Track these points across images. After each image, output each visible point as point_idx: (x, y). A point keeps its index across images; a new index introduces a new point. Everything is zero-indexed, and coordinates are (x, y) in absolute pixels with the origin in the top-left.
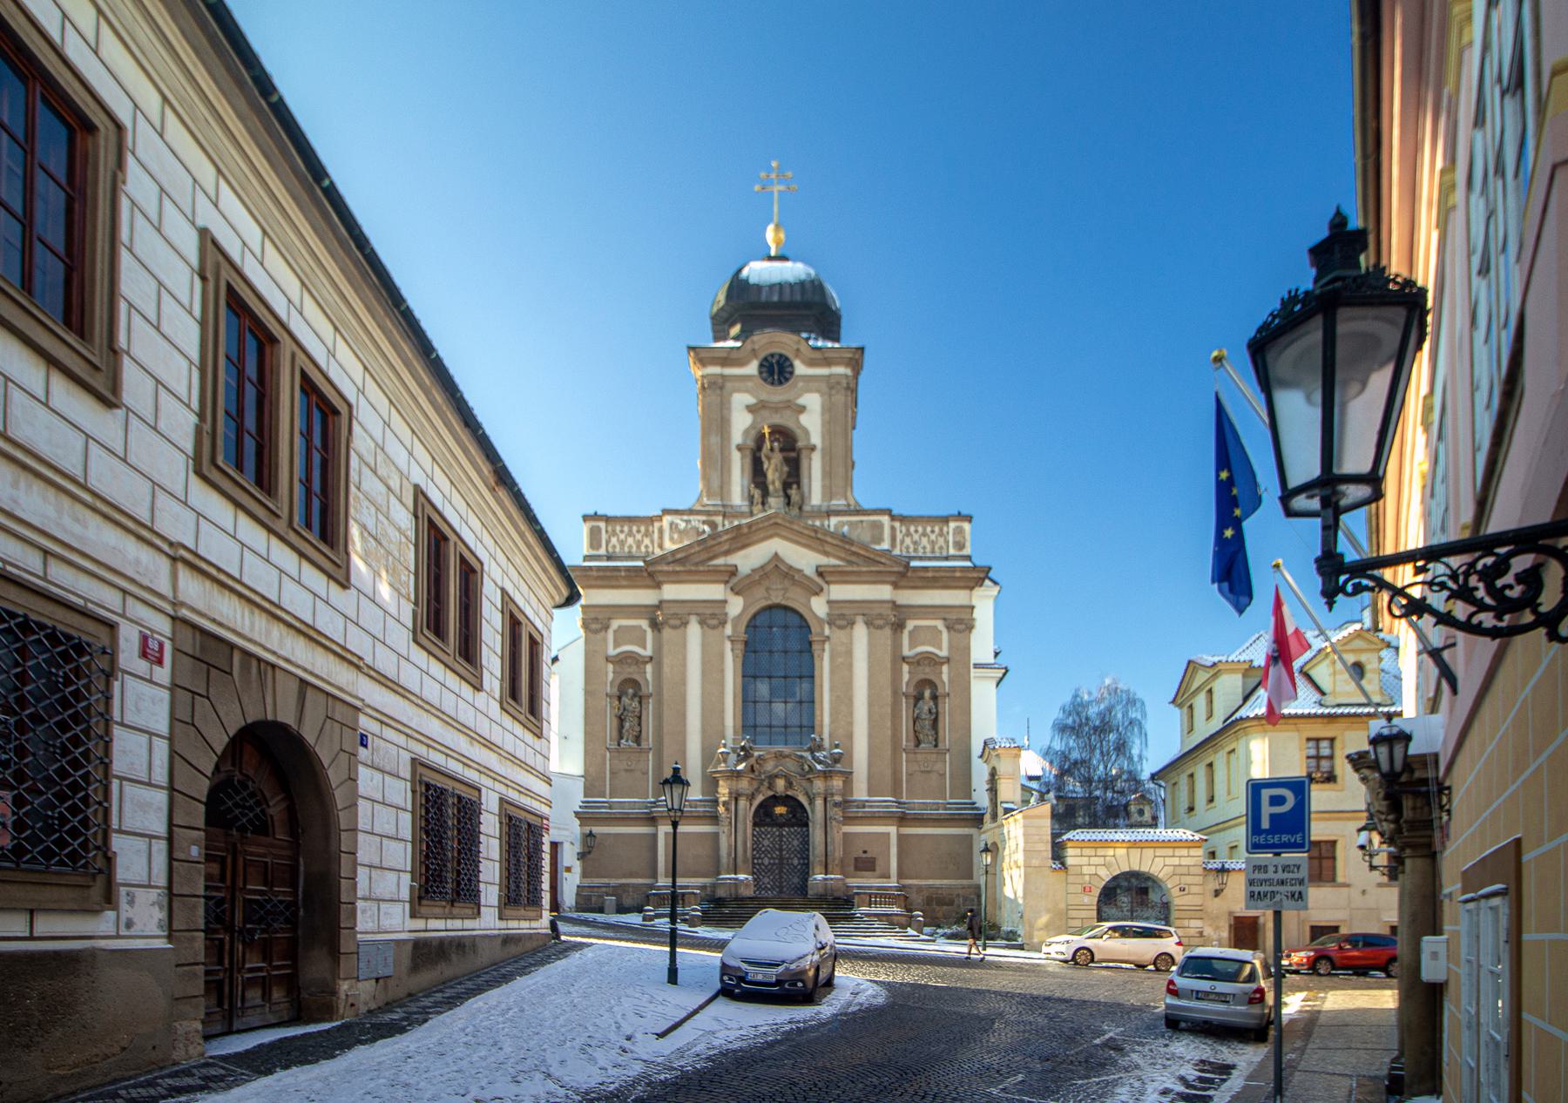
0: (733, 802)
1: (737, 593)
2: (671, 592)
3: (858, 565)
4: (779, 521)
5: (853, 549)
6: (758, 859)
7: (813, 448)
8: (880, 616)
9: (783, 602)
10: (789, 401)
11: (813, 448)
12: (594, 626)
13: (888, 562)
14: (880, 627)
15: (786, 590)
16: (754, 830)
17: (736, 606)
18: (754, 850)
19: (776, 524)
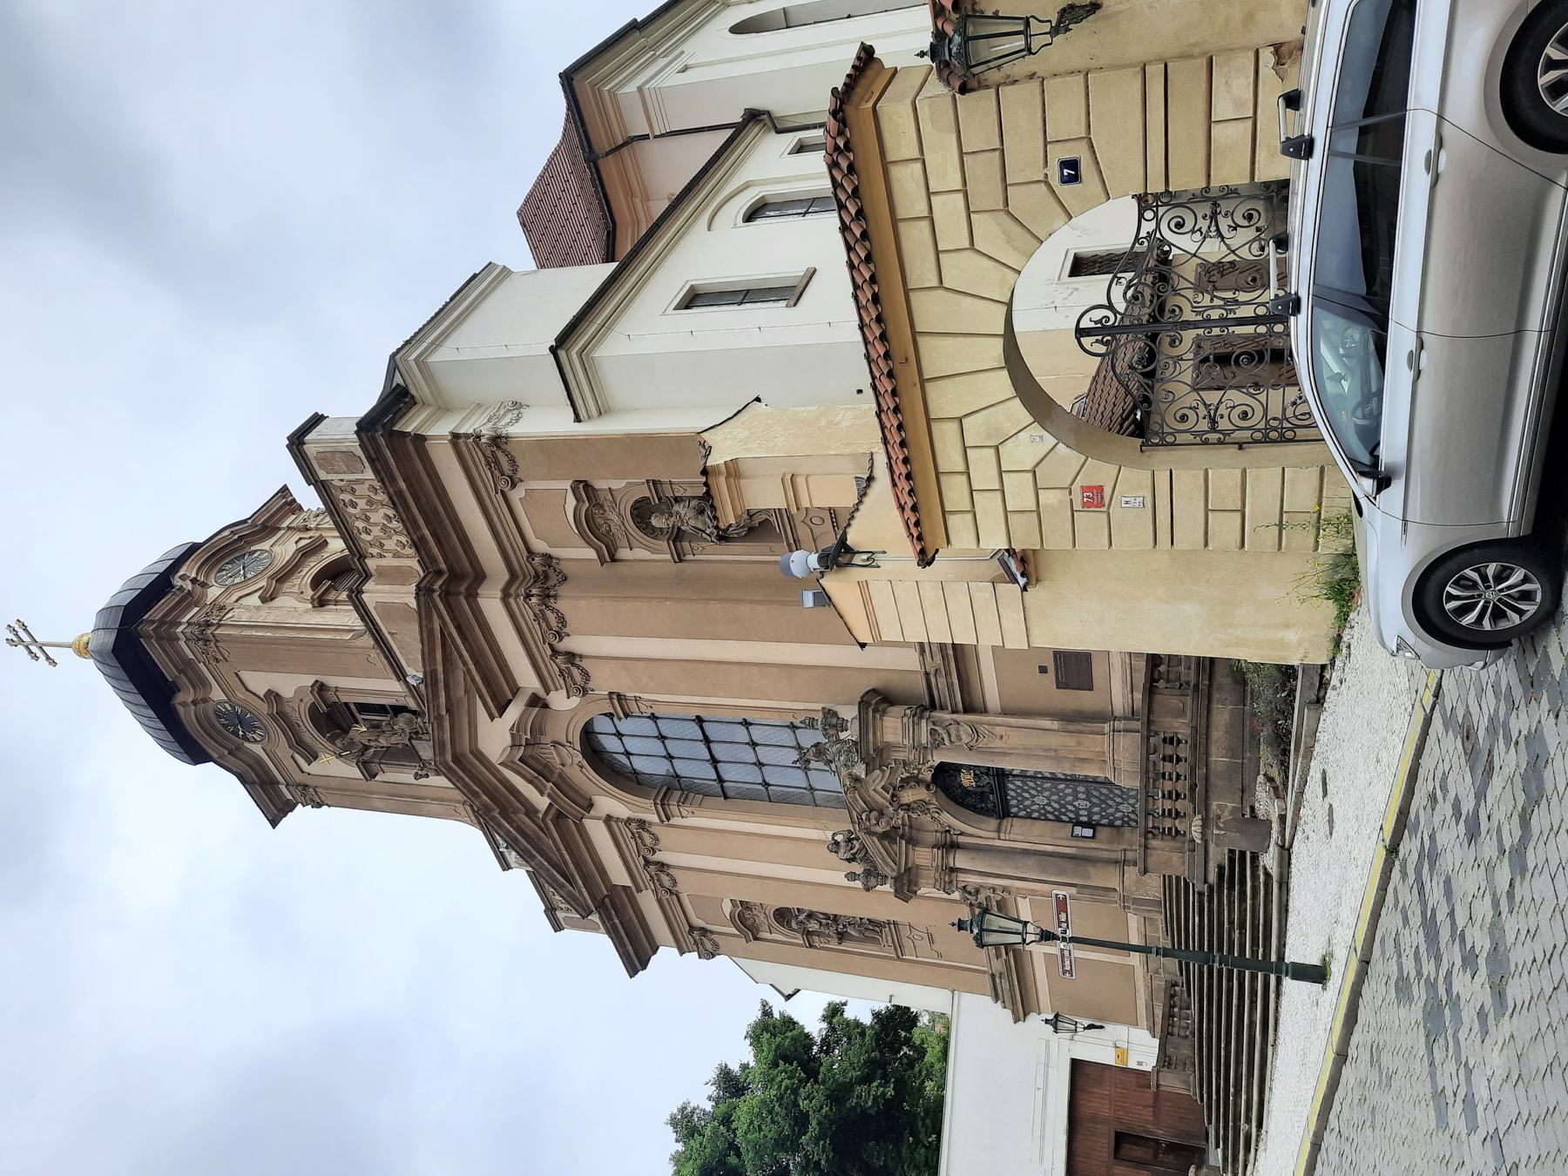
0: (962, 877)
1: (591, 805)
2: (620, 876)
3: (465, 664)
4: (449, 757)
5: (440, 668)
6: (1078, 815)
7: (320, 688)
8: (540, 617)
9: (578, 747)
10: (271, 715)
11: (320, 688)
12: (709, 945)
13: (435, 617)
14: (562, 620)
15: (556, 743)
16: (1016, 816)
17: (611, 803)
18: (1058, 820)
19: (456, 759)
